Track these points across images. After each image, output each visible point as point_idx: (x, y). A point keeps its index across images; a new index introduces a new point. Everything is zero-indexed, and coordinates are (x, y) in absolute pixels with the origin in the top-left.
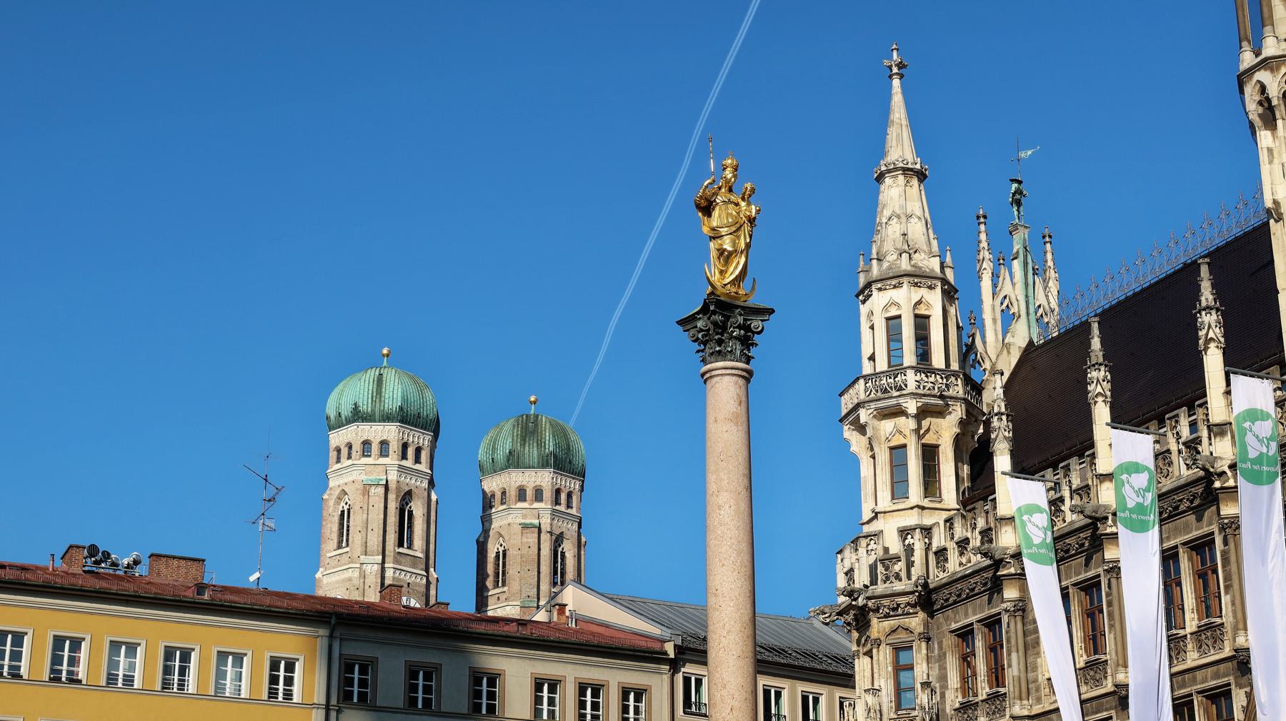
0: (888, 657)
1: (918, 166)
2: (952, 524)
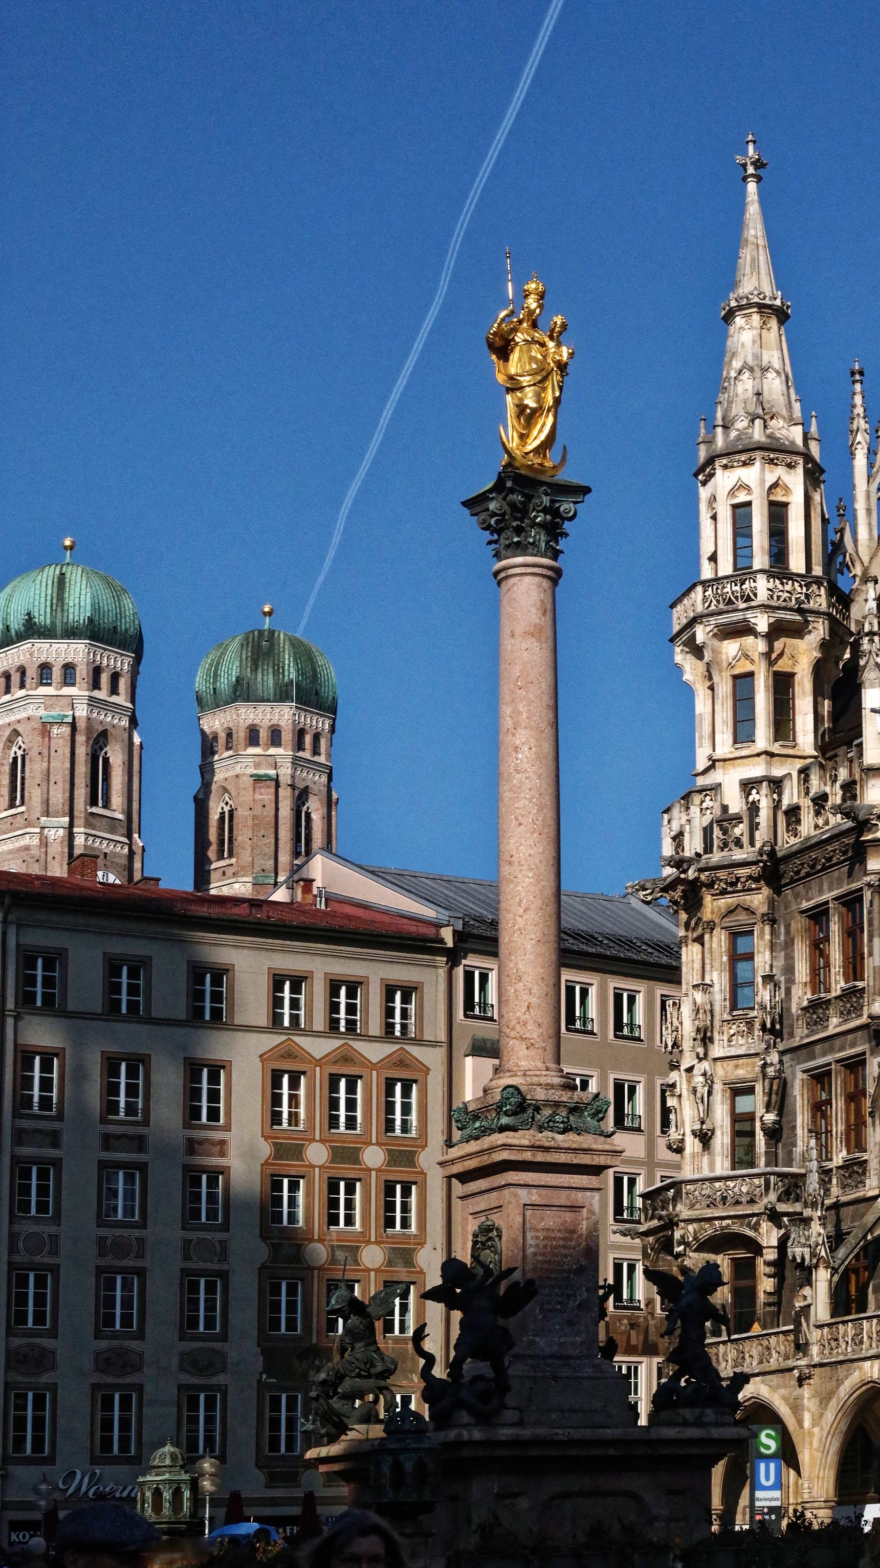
0: (723, 943)
2: (807, 776)
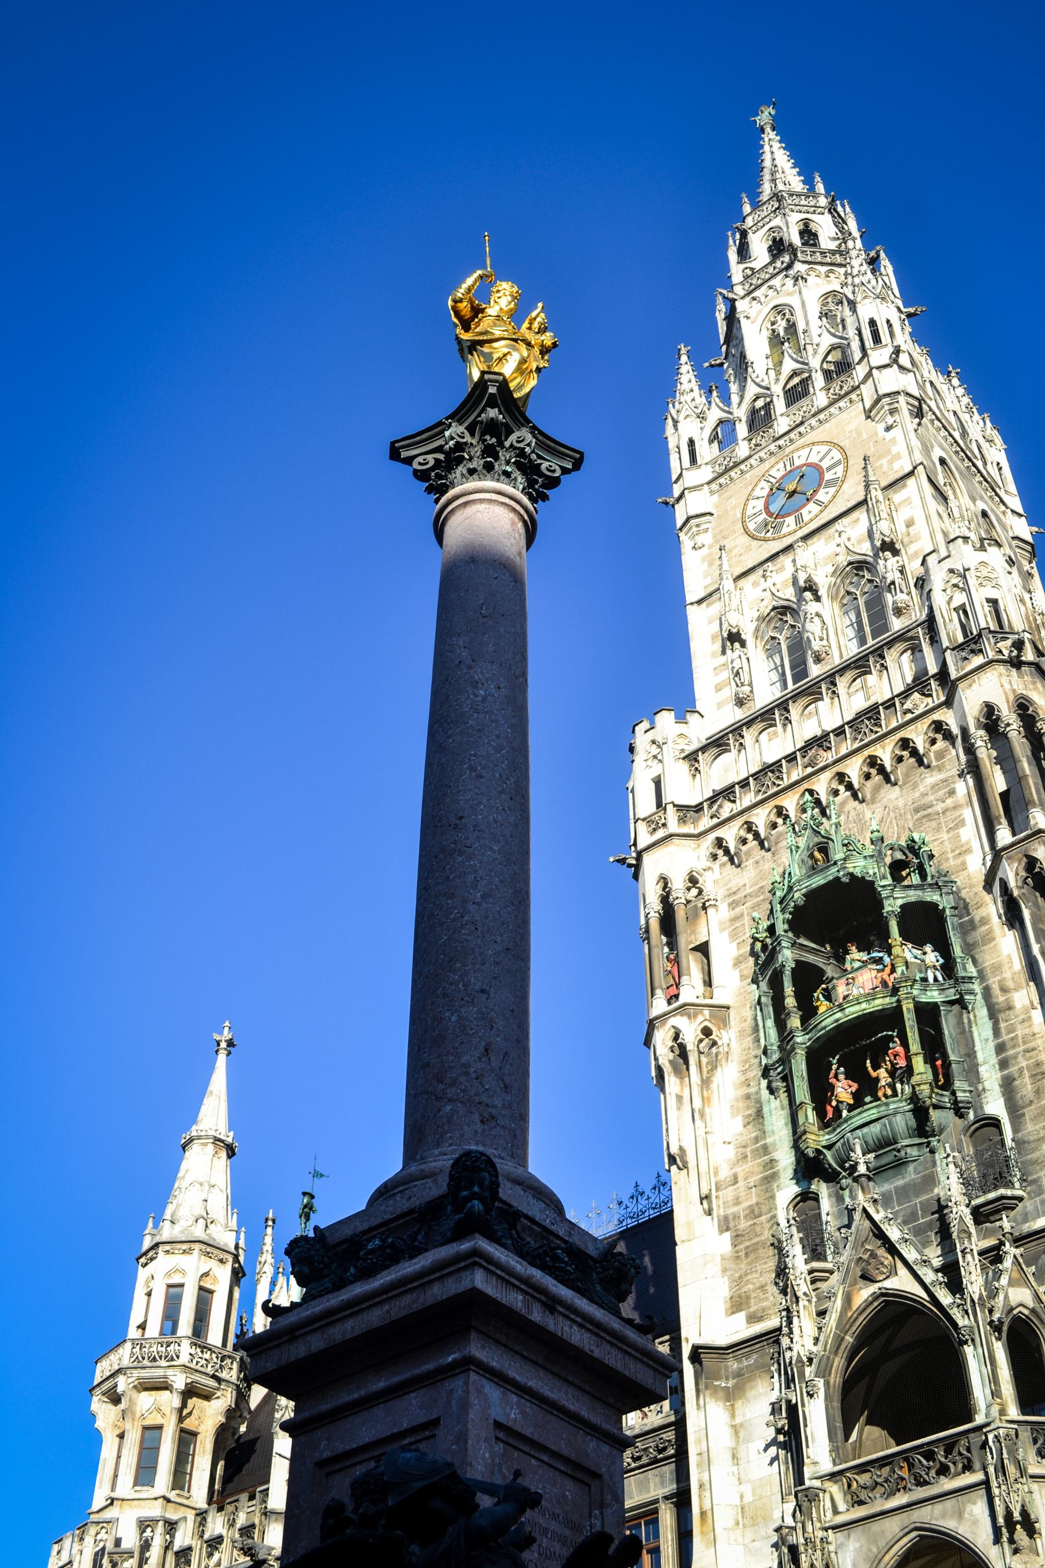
1: (230, 1140)
2: (205, 1519)
